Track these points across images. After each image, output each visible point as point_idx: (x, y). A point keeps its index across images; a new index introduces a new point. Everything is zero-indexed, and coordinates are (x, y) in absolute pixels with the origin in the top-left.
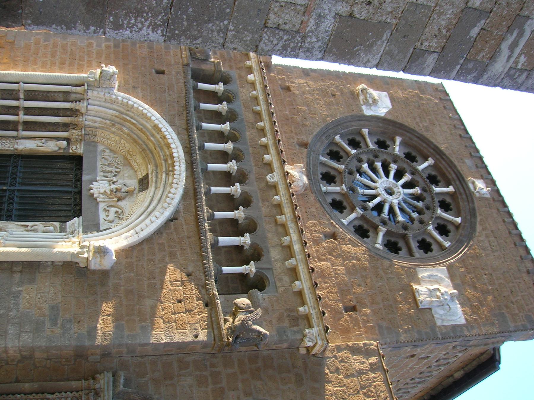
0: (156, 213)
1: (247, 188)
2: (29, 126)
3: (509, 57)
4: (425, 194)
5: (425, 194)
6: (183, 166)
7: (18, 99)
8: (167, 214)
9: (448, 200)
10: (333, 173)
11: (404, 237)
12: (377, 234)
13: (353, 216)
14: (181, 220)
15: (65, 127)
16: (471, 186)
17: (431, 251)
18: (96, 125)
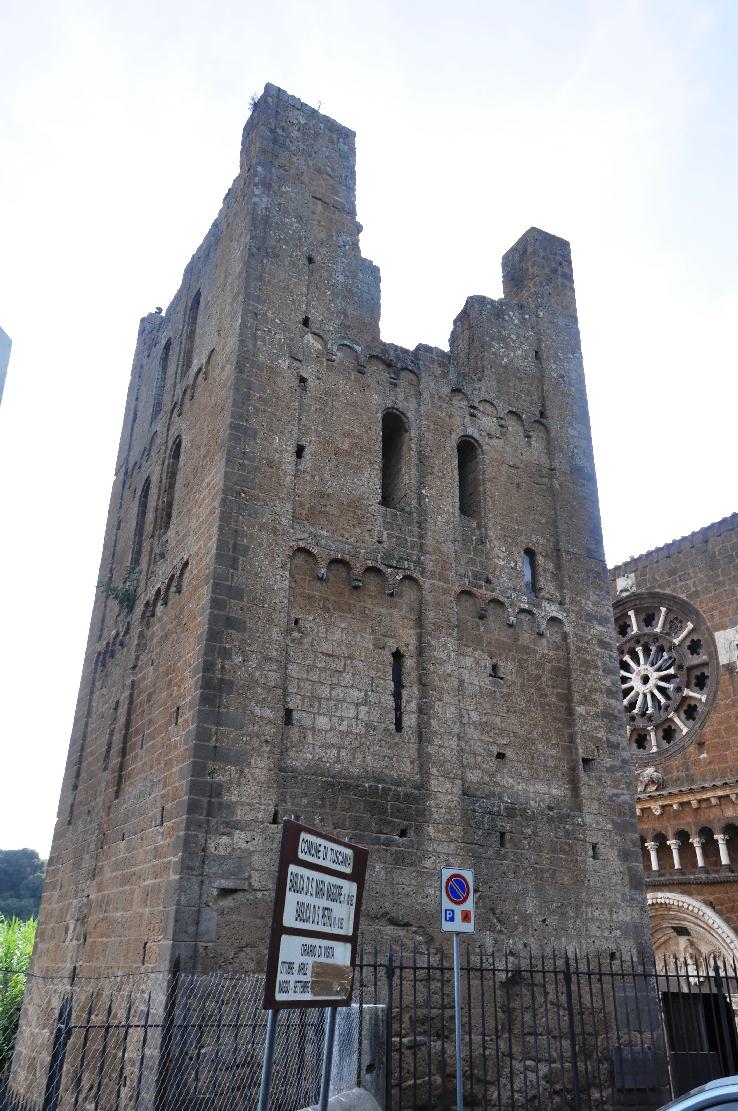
0: (710, 922)
1: (670, 834)
3: (623, 794)
4: (642, 642)
5: (642, 642)
6: (660, 895)
8: (709, 912)
9: (643, 616)
10: (635, 737)
11: (690, 669)
12: (691, 697)
13: (676, 720)
14: (711, 898)
16: (625, 594)
17: (699, 641)
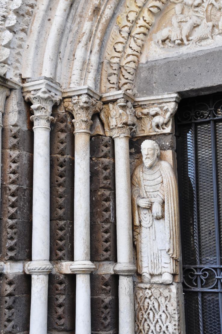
2: (103, 246)
7: (26, 279)
15: (100, 147)
18: (94, 59)
